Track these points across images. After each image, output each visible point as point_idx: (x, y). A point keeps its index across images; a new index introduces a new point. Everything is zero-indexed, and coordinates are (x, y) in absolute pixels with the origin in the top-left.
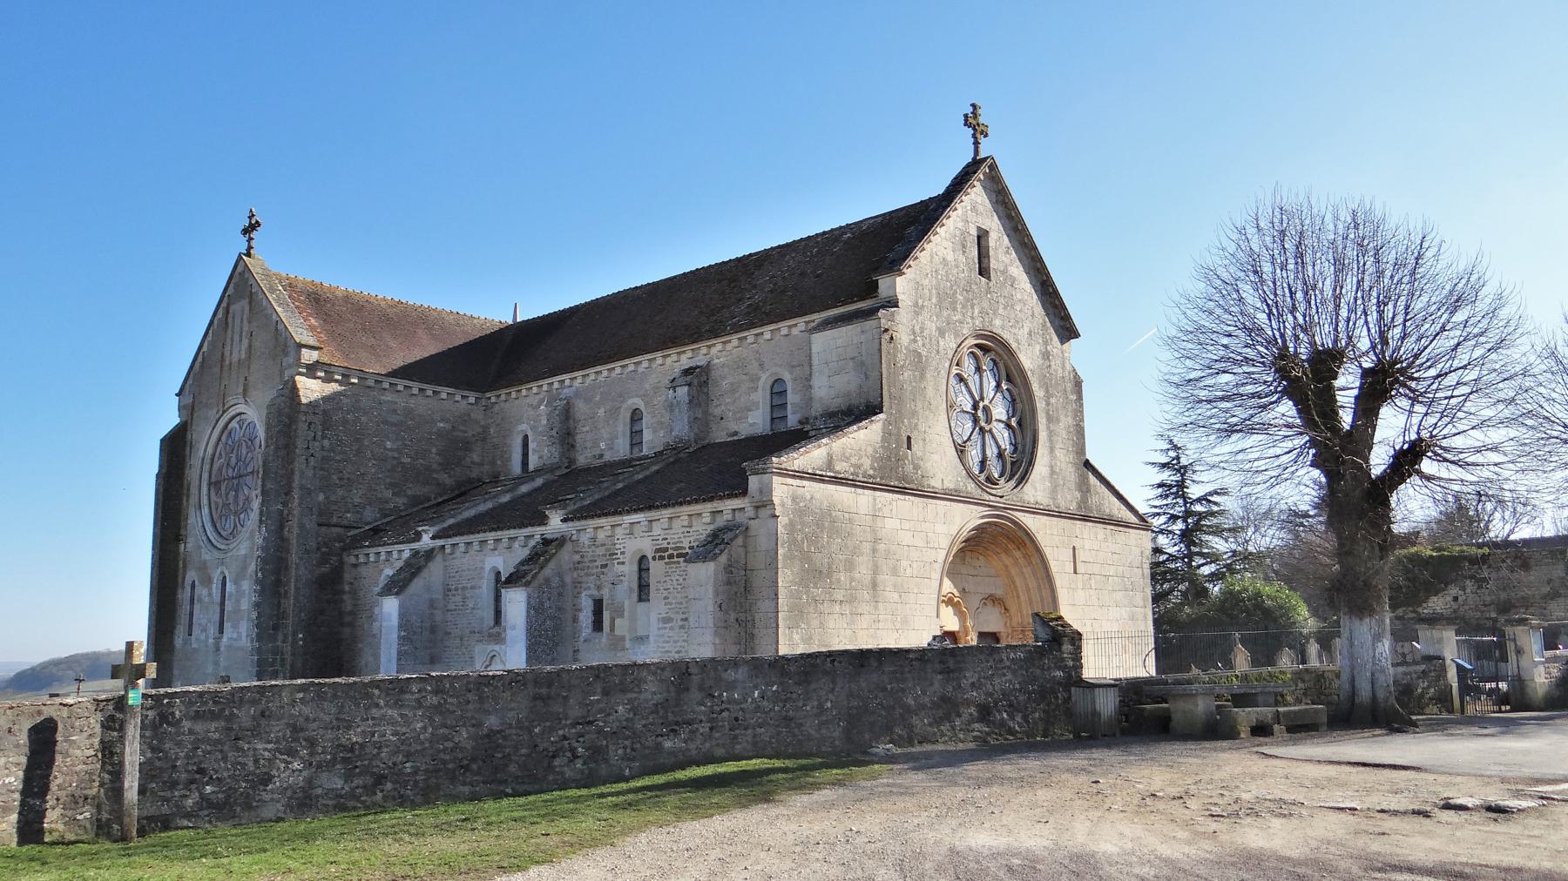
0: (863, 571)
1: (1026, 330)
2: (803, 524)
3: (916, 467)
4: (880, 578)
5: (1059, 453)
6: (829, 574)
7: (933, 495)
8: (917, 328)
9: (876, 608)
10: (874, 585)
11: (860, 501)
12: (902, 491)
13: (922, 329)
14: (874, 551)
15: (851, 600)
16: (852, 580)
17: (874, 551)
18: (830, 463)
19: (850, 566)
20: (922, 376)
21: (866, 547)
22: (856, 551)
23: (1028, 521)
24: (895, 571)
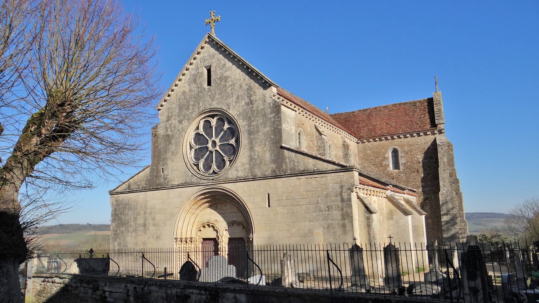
0: (140, 221)
1: (235, 97)
2: (119, 209)
3: (165, 179)
4: (147, 222)
5: (257, 148)
6: (128, 224)
7: (173, 187)
8: (168, 126)
9: (145, 233)
10: (145, 225)
11: (141, 196)
12: (157, 189)
13: (170, 125)
14: (145, 213)
15: (135, 230)
16: (136, 224)
17: (145, 213)
18: (129, 187)
19: (135, 219)
20: (170, 143)
21: (142, 212)
22: (138, 214)
23: (230, 187)
24: (154, 219)
